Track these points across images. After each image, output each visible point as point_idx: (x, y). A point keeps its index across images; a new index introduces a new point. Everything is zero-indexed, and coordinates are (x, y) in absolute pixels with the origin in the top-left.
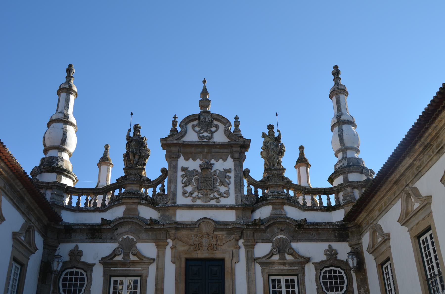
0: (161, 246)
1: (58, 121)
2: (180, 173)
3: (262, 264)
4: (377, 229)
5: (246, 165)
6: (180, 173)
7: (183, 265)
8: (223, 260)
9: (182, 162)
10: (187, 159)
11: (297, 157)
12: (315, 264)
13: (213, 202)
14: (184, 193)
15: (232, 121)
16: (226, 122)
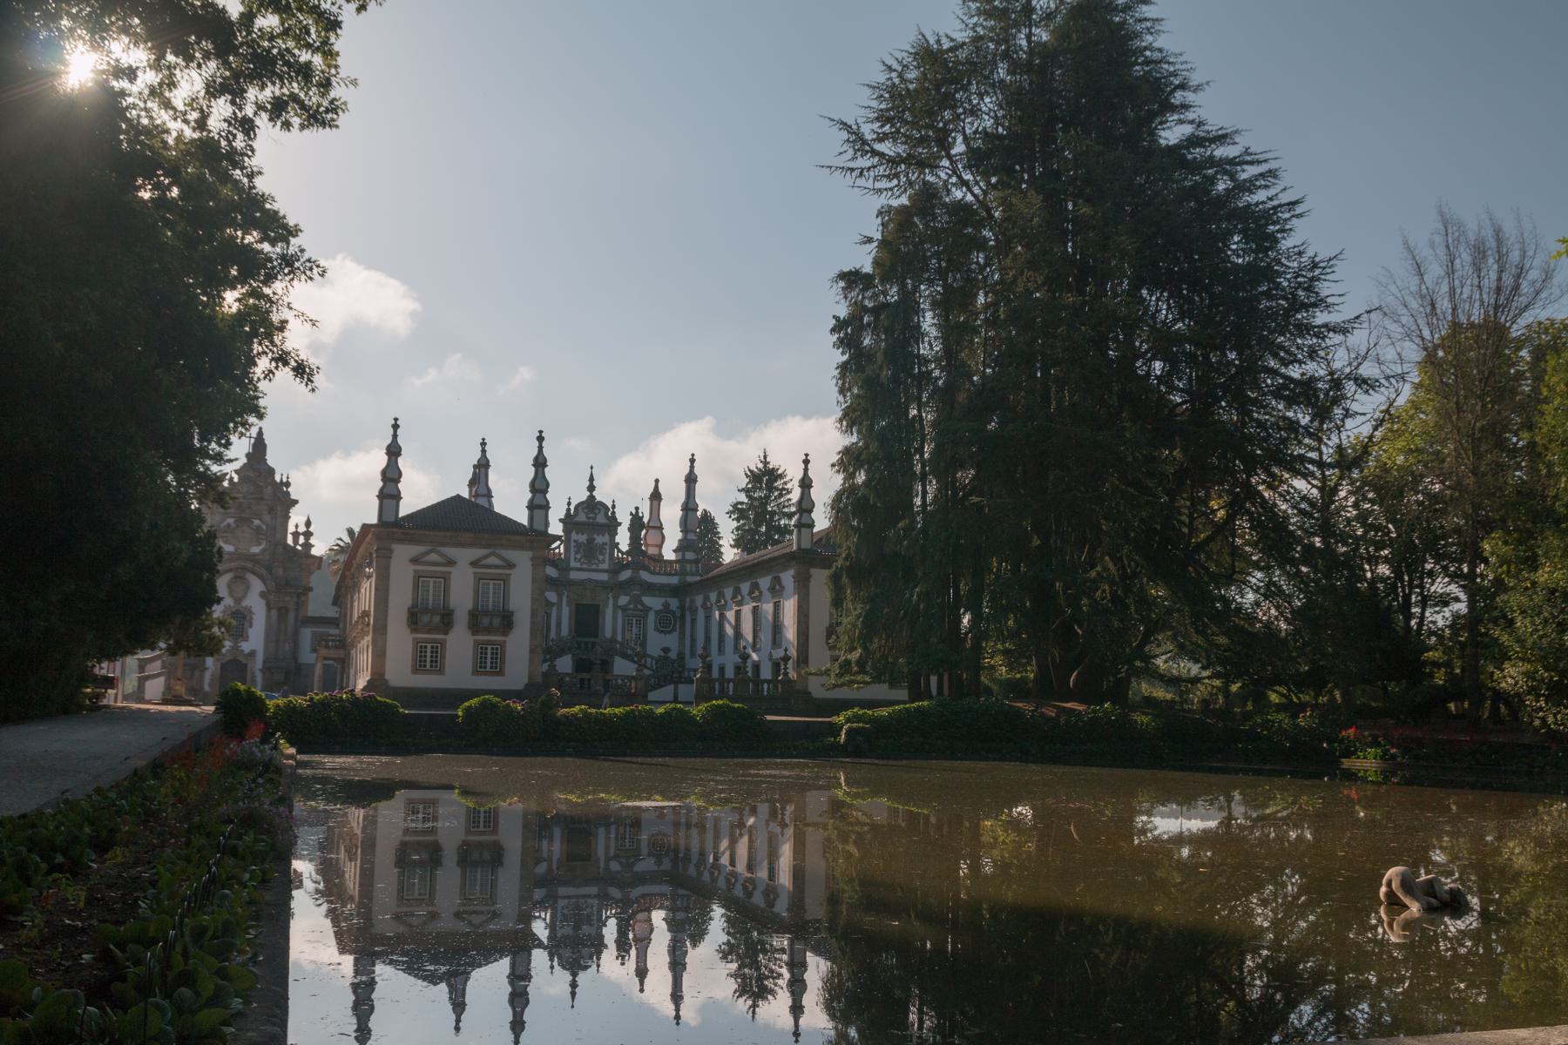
0: (560, 596)
1: (484, 496)
2: (573, 544)
3: (622, 609)
4: (692, 601)
5: (617, 539)
6: (573, 544)
7: (574, 606)
8: (598, 605)
9: (574, 536)
10: (577, 533)
11: (652, 490)
12: (656, 612)
13: (594, 567)
14: (575, 558)
15: (610, 507)
16: (607, 508)
